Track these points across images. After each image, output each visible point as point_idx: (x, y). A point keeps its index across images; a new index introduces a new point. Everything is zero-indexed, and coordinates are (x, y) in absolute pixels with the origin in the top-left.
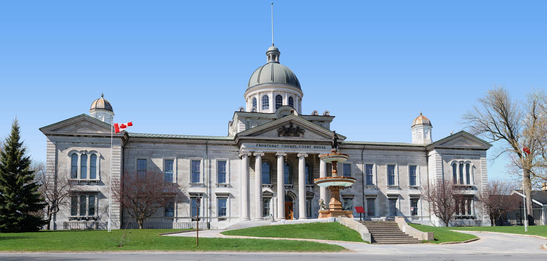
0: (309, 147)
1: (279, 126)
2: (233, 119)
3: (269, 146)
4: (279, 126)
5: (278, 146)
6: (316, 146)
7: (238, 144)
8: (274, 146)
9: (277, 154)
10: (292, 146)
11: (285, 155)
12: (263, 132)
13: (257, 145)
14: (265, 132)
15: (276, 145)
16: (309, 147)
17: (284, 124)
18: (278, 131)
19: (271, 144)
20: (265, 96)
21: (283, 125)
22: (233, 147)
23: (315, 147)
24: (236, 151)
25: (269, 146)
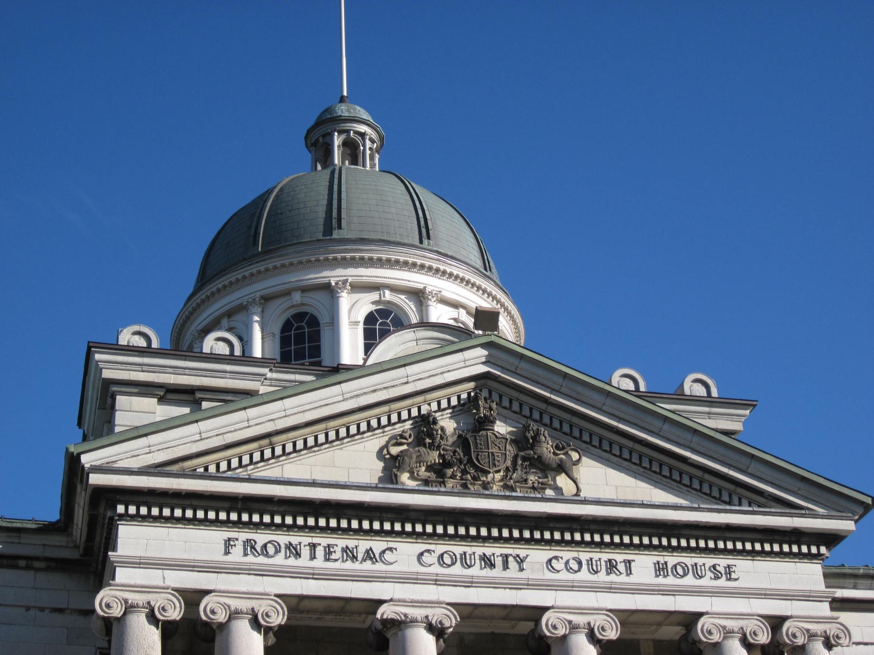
0: (621, 567)
1: (394, 418)
2: (80, 424)
3: (320, 552)
4: (394, 418)
5: (388, 556)
6: (672, 560)
7: (88, 550)
8: (360, 557)
9: (385, 612)
10: (499, 561)
11: (451, 621)
12: (278, 451)
13: (228, 544)
14: (295, 450)
15: (378, 545)
16: (621, 567)
17: (434, 406)
18: (380, 455)
19: (340, 542)
20: (300, 316)
21: (425, 410)
22: (57, 579)
23: (661, 569)
24: (73, 606)
25: (320, 552)
